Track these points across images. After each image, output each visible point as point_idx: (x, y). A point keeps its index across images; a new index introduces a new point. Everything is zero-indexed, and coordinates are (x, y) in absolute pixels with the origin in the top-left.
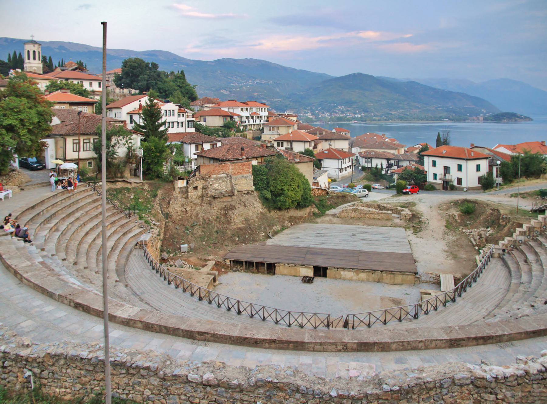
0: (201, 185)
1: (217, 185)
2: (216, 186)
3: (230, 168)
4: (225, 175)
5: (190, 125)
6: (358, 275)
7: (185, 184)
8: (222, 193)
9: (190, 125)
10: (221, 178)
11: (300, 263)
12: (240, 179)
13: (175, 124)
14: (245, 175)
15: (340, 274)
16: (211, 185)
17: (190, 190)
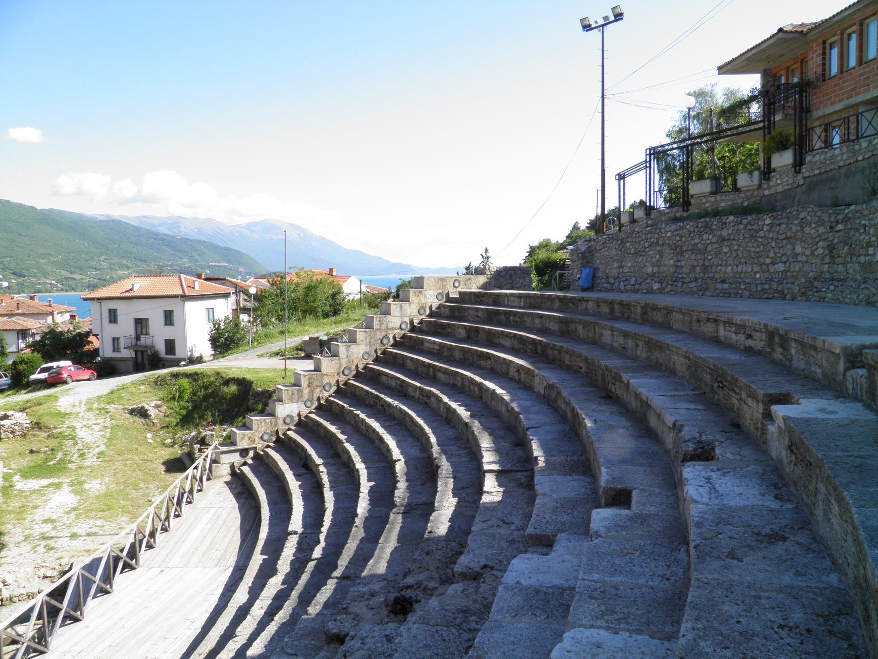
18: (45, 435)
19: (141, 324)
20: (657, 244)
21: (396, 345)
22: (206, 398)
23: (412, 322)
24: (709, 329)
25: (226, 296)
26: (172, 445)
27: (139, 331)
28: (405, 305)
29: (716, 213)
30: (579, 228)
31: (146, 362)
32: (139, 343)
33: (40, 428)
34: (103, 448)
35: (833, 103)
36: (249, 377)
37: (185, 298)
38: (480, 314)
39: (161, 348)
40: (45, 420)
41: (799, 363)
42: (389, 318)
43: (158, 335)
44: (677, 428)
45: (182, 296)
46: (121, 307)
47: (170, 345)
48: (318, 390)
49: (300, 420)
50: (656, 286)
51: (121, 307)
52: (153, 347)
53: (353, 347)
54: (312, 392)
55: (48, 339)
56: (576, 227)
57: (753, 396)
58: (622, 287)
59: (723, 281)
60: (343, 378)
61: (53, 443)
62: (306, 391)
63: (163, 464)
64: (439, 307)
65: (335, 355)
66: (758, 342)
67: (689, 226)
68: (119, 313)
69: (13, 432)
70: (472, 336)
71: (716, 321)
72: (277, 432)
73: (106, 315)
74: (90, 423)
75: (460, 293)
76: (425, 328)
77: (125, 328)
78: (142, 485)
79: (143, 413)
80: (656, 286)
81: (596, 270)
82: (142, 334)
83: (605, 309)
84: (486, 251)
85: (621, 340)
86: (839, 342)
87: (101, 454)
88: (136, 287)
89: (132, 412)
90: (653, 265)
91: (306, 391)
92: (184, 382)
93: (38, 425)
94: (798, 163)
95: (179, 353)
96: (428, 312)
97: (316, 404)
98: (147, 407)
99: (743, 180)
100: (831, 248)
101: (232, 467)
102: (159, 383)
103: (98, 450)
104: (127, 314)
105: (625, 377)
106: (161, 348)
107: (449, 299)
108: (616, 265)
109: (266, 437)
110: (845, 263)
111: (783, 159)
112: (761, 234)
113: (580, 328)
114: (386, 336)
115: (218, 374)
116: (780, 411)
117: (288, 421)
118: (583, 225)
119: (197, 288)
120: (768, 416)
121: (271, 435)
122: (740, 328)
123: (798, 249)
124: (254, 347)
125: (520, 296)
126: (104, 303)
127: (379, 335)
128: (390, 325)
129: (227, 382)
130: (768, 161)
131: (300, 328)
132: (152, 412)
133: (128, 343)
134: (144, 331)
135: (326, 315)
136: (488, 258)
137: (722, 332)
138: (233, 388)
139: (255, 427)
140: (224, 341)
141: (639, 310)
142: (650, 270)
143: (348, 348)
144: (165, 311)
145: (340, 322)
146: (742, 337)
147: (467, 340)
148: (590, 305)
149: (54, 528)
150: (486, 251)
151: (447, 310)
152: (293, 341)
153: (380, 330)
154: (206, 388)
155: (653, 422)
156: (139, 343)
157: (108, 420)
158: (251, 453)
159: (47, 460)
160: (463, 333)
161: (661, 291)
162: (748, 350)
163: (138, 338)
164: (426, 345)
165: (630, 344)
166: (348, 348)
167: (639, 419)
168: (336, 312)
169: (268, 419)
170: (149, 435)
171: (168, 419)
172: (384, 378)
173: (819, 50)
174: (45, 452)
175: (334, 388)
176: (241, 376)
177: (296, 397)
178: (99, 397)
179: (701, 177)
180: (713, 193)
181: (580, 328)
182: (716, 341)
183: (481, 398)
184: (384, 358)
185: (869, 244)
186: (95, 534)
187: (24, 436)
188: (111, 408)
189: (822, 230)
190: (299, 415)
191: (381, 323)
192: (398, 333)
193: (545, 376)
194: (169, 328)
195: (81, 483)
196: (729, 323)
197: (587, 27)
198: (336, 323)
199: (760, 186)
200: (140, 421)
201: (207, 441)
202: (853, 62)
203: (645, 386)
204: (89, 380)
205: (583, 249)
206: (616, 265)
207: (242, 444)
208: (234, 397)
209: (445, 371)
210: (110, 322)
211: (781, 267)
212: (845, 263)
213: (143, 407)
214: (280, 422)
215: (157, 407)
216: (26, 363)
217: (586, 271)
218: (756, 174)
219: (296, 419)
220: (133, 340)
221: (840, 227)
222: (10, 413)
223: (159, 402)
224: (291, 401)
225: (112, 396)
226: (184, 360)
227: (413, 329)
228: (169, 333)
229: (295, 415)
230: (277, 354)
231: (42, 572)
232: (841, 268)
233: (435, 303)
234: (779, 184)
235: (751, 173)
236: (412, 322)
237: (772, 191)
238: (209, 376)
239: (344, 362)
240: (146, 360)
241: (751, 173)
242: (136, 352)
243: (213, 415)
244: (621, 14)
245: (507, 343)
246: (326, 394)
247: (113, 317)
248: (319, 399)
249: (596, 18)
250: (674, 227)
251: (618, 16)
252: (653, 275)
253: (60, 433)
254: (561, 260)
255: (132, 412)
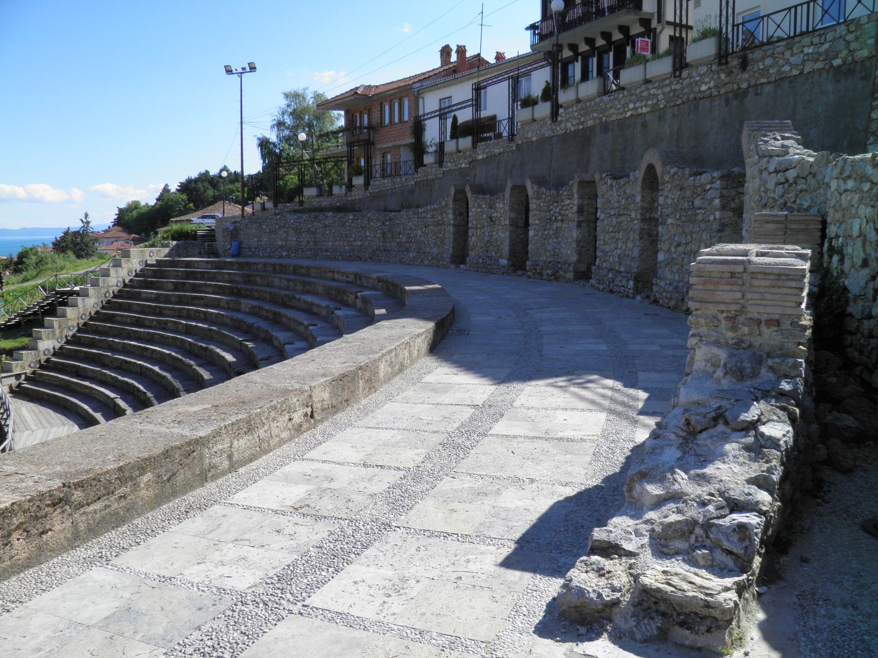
20: (284, 227)
21: (115, 296)
23: (124, 282)
24: (330, 275)
28: (119, 269)
29: (322, 210)
30: (168, 191)
35: (387, 142)
38: (179, 274)
41: (365, 284)
42: (109, 279)
44: (327, 307)
48: (65, 330)
49: (55, 352)
50: (284, 254)
53: (87, 300)
54: (61, 332)
56: (166, 190)
57: (351, 293)
58: (261, 254)
59: (327, 251)
60: (82, 322)
62: (57, 332)
64: (141, 270)
65: (75, 305)
66: (351, 279)
67: (305, 216)
70: (177, 287)
71: (333, 272)
72: (40, 361)
75: (157, 261)
76: (135, 284)
80: (284, 254)
81: (241, 243)
83: (270, 268)
84: (86, 215)
85: (286, 283)
86: (375, 276)
90: (282, 240)
91: (57, 332)
94: (367, 184)
96: (134, 274)
97: (65, 340)
99: (336, 190)
100: (384, 234)
101: (11, 387)
105: (298, 297)
107: (147, 265)
108: (255, 239)
109: (32, 365)
110: (390, 242)
111: (359, 181)
112: (348, 224)
113: (258, 279)
114: (108, 292)
116: (359, 294)
117: (46, 352)
118: (174, 187)
120: (357, 297)
121: (35, 363)
122: (344, 274)
123: (368, 233)
125: (207, 262)
127: (103, 291)
128: (110, 284)
130: (350, 180)
136: (88, 223)
137: (336, 276)
139: (24, 358)
141: (292, 268)
142: (280, 243)
143: (83, 300)
146: (344, 277)
147: (176, 290)
148: (260, 266)
150: (86, 215)
151: (150, 272)
153: (103, 287)
155: (315, 309)
158: (23, 377)
160: (171, 286)
161: (288, 256)
162: (348, 282)
164: (143, 295)
165: (291, 284)
166: (83, 300)
167: (308, 310)
169: (33, 352)
172: (119, 318)
173: (379, 108)
175: (76, 329)
177: (51, 336)
179: (310, 185)
180: (318, 196)
181: (258, 279)
182: (334, 280)
183: (206, 320)
184: (109, 305)
185: (400, 233)
189: (379, 224)
190: (54, 348)
191: (104, 282)
192: (116, 289)
193: (246, 304)
196: (339, 272)
197: (229, 71)
199: (346, 194)
202: (397, 120)
203: (309, 298)
205: (231, 228)
206: (255, 239)
207: (17, 371)
209: (172, 309)
211: (359, 243)
212: (390, 242)
214: (42, 353)
217: (234, 244)
218: (344, 187)
219: (52, 351)
221: (387, 223)
224: (48, 339)
227: (125, 285)
229: (51, 348)
232: (388, 245)
233: (139, 268)
234: (357, 194)
235: (341, 186)
236: (124, 282)
237: (353, 198)
239: (81, 310)
241: (341, 186)
244: (255, 68)
245: (210, 289)
246: (71, 333)
248: (66, 337)
249: (236, 66)
250: (295, 217)
251: (253, 68)
252: (282, 247)
254: (192, 231)
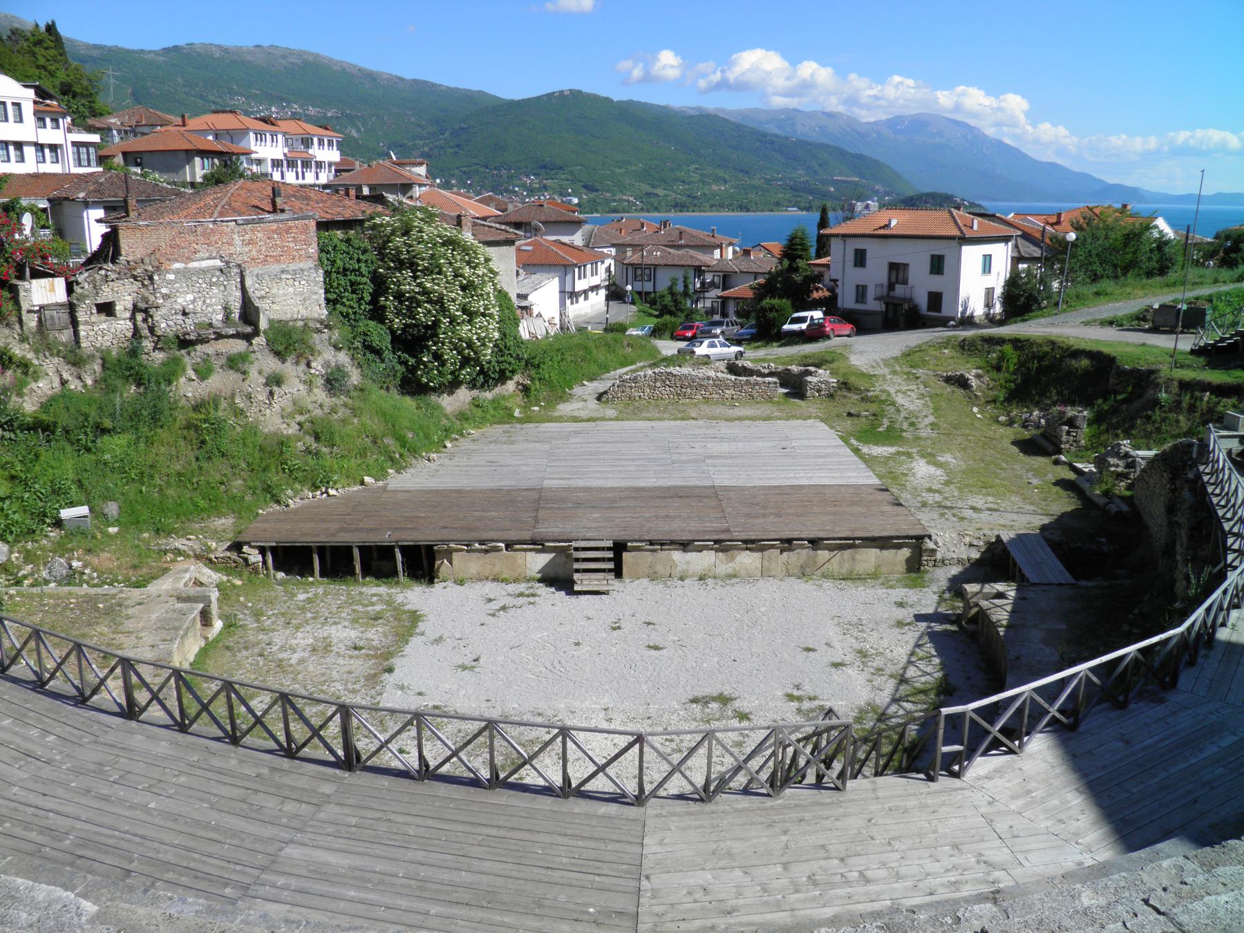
0: (124, 296)
1: (190, 297)
2: (185, 299)
3: (237, 239)
4: (218, 263)
5: (83, 157)
6: (733, 559)
7: (60, 295)
8: (211, 325)
9: (83, 157)
10: (204, 271)
11: (526, 535)
12: (277, 278)
13: (29, 152)
14: (292, 267)
15: (674, 564)
16: (166, 297)
17: (81, 316)
18: (856, 397)
19: (897, 270)
22: (1040, 370)
25: (1005, 239)
26: (1011, 423)
27: (893, 279)
31: (902, 319)
32: (892, 294)
33: (849, 390)
34: (931, 419)
36: (1106, 350)
37: (965, 240)
39: (922, 301)
40: (852, 380)
43: (920, 285)
45: (960, 238)
46: (872, 248)
47: (935, 300)
51: (872, 248)
52: (910, 300)
55: (780, 282)
61: (873, 407)
63: (1014, 443)
68: (869, 255)
69: (819, 391)
73: (850, 257)
74: (904, 388)
77: (875, 274)
78: (1004, 465)
79: (962, 383)
82: (897, 282)
87: (933, 426)
88: (894, 223)
89: (948, 380)
92: (1008, 348)
93: (845, 385)
95: (946, 311)
98: (967, 375)
101: (1229, 453)
102: (965, 347)
103: (927, 421)
104: (879, 258)
106: (922, 301)
115: (1053, 343)
119: (975, 227)
124: (1064, 311)
126: (849, 240)
129: (1076, 354)
131: (1140, 293)
132: (974, 383)
133: (879, 294)
134: (901, 276)
135: (1149, 274)
138: (1085, 362)
140: (1019, 300)
144: (933, 256)
145: (1174, 284)
149: (946, 499)
152: (1135, 305)
154: (1041, 358)
156: (892, 294)
157: (922, 386)
159: (873, 426)
163: (891, 287)
168: (1163, 271)
170: (975, 410)
171: (991, 393)
174: (866, 417)
176: (1094, 348)
178: (896, 359)
186: (996, 510)
187: (831, 396)
188: (920, 372)
194: (936, 278)
195: (932, 455)
198: (1168, 286)
200: (960, 392)
201: (1078, 423)
204: (848, 336)
208: (1087, 373)
210: (855, 265)
213: (962, 375)
215: (978, 376)
216: (777, 311)
220: (885, 290)
222: (812, 369)
223: (980, 371)
225: (910, 357)
226: (953, 319)
228: (935, 283)
230: (1111, 323)
231: (967, 540)
238: (1040, 345)
240: (898, 314)
242: (887, 304)
243: (1059, 393)
247: (860, 258)
253: (876, 397)
255: (948, 380)
